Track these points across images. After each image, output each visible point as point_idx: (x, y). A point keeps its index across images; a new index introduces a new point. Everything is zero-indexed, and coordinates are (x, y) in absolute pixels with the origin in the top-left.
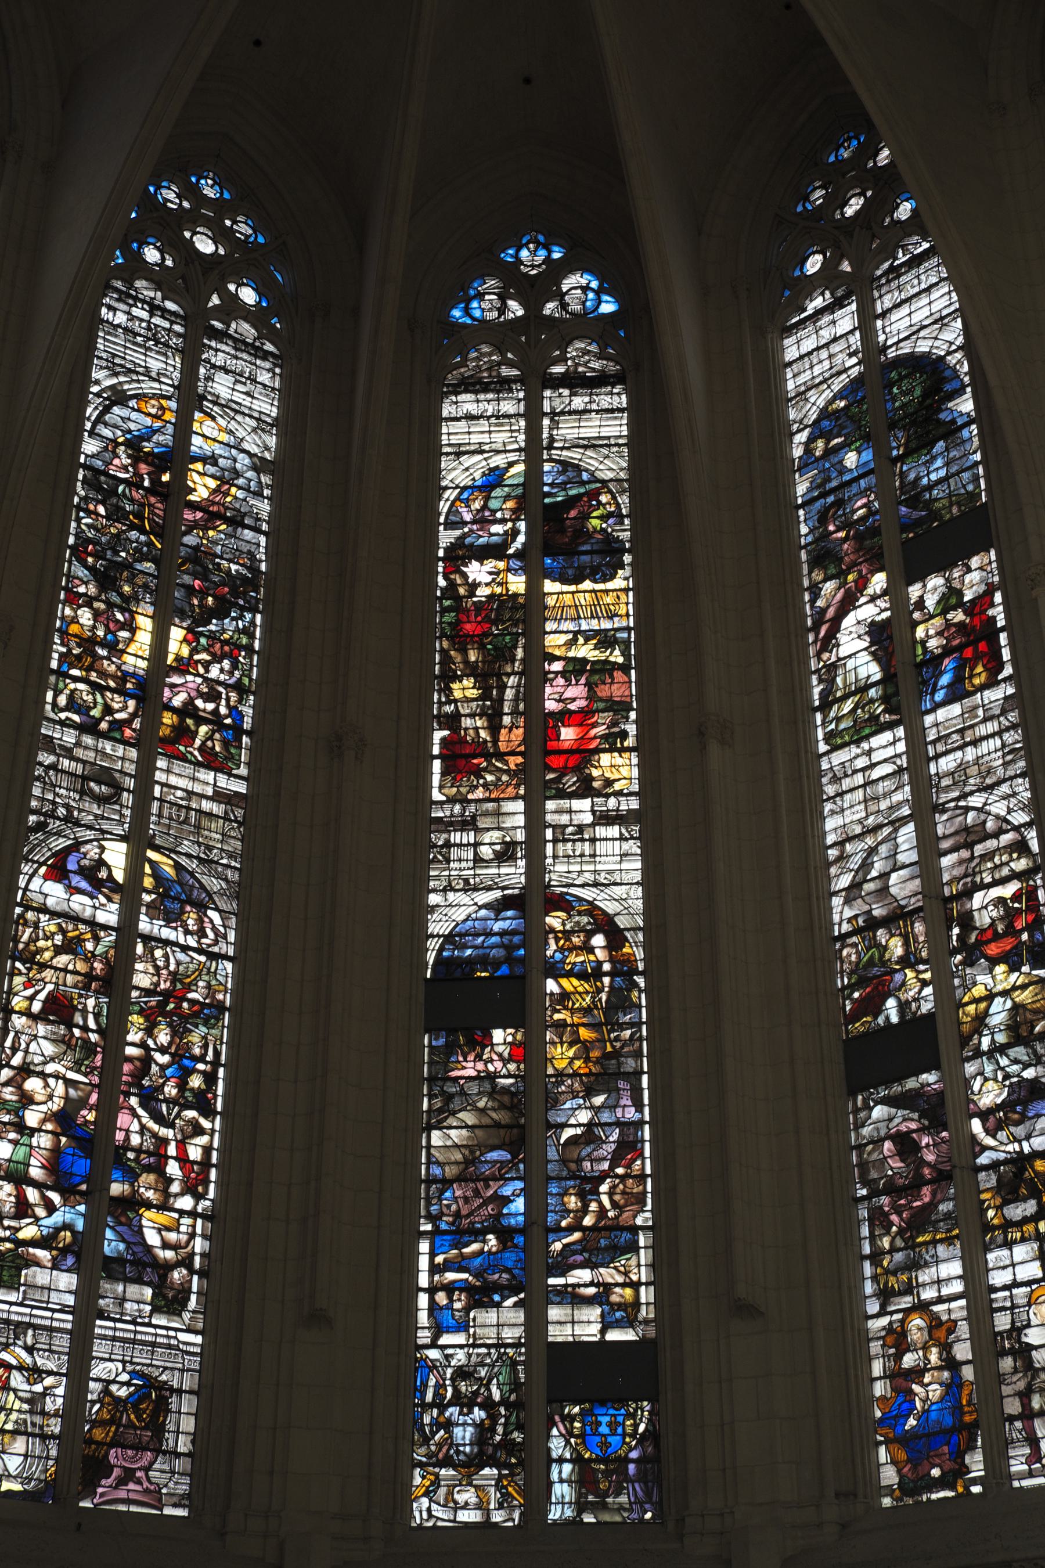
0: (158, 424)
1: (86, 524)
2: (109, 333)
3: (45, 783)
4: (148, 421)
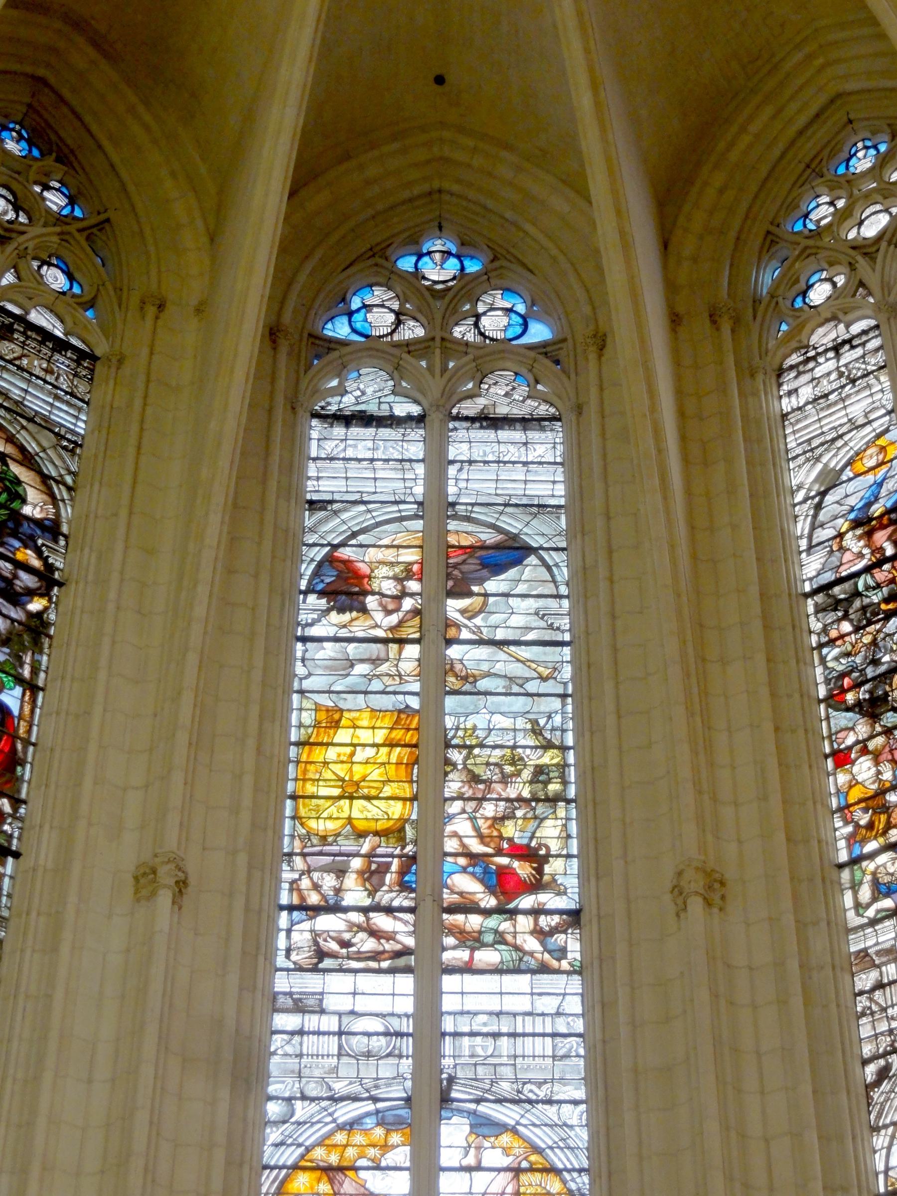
0: (881, 472)
1: (836, 659)
2: (798, 421)
3: (872, 1014)
4: (870, 478)
